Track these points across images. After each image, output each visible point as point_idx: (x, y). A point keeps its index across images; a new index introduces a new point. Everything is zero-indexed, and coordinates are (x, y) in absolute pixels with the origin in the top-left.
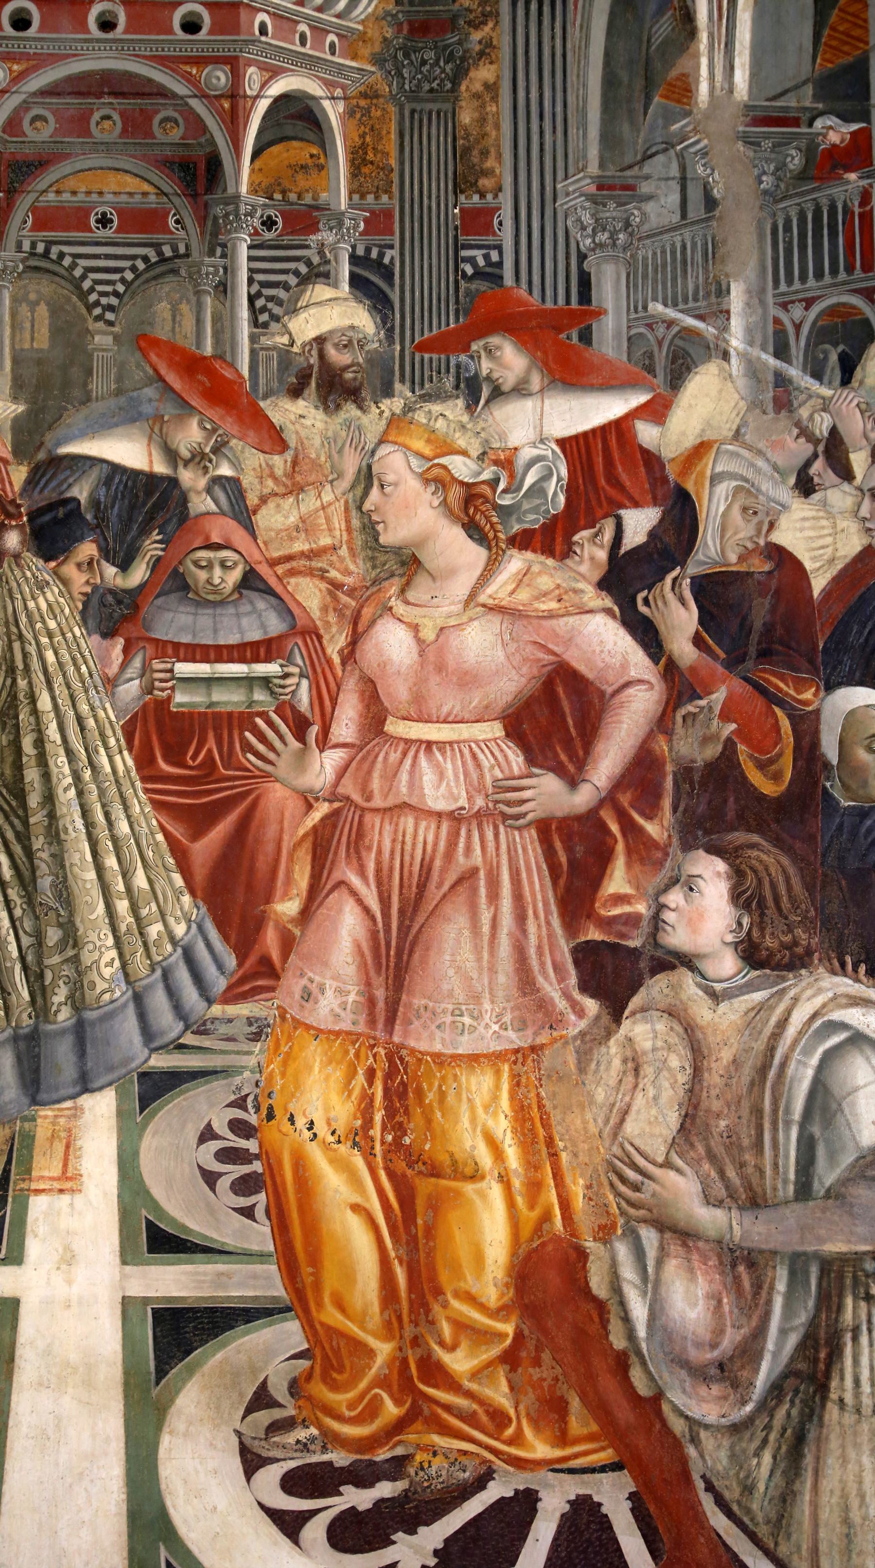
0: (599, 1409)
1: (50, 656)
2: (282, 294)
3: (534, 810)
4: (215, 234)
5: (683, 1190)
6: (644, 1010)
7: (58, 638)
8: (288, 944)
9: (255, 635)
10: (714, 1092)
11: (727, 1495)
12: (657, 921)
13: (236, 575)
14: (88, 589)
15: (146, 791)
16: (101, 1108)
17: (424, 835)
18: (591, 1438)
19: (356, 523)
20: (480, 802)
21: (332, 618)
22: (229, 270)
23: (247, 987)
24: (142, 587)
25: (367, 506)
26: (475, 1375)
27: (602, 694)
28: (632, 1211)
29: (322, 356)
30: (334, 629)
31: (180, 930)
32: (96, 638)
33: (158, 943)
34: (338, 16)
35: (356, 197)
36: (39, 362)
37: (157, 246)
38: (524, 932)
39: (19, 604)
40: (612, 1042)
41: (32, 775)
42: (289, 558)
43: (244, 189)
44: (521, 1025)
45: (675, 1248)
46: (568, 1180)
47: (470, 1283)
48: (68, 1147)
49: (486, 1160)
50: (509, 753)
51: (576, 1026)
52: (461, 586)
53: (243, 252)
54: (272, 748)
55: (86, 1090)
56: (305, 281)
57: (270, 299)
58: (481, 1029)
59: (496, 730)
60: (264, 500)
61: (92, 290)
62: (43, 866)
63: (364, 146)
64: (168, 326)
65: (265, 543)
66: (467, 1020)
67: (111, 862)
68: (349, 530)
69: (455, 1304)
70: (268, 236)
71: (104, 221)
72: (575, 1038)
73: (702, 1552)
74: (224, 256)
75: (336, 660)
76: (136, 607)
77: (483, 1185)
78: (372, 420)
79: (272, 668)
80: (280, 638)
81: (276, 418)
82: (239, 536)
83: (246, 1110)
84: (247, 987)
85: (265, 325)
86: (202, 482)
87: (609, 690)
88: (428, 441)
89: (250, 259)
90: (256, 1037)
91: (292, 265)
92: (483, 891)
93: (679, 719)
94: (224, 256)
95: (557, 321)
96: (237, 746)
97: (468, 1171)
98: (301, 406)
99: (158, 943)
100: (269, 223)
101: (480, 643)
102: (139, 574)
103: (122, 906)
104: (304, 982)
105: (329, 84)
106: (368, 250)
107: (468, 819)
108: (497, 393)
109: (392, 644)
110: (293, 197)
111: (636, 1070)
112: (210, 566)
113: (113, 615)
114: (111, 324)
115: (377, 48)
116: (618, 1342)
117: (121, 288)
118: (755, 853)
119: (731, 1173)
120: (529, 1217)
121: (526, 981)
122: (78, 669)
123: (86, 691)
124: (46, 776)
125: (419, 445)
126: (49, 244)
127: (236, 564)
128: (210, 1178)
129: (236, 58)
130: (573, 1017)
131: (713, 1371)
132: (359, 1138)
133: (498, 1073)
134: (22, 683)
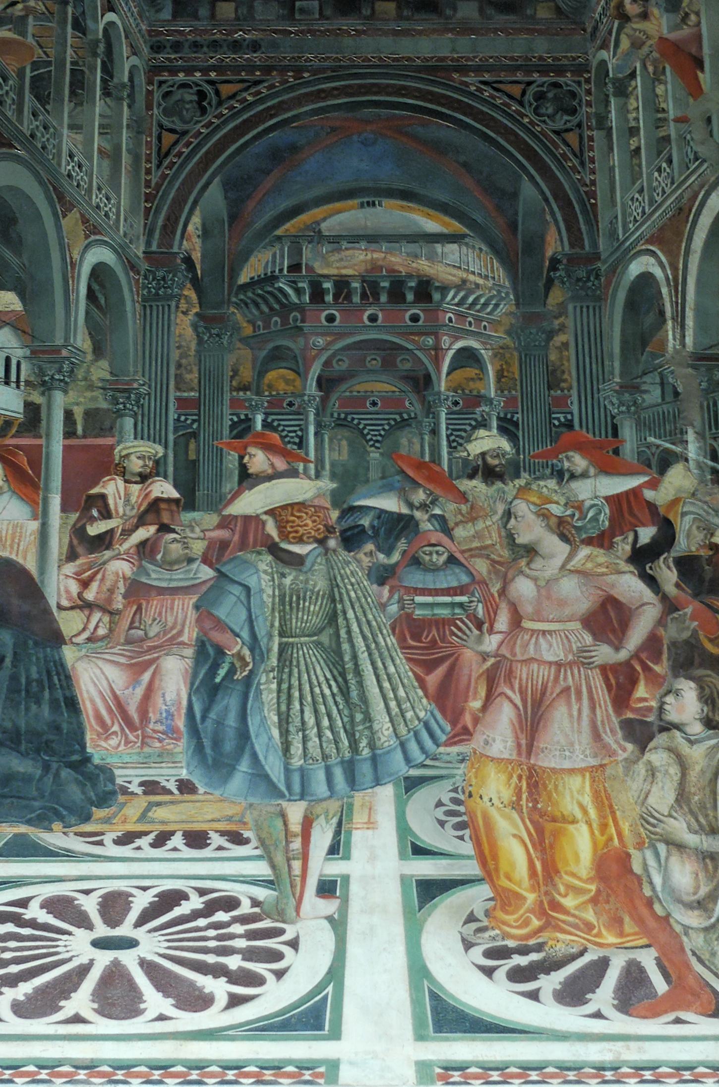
0: (639, 921)
1: (353, 594)
2: (463, 434)
3: (598, 661)
4: (430, 407)
5: (679, 827)
6: (655, 748)
7: (356, 586)
8: (476, 721)
9: (455, 584)
10: (692, 784)
11: (703, 957)
12: (661, 710)
13: (444, 557)
14: (370, 564)
15: (403, 653)
16: (386, 794)
17: (542, 674)
18: (635, 934)
19: (503, 534)
20: (570, 657)
21: (493, 576)
22: (437, 424)
23: (456, 739)
24: (397, 564)
25: (509, 526)
26: (577, 908)
27: (630, 609)
28: (652, 836)
29: (484, 460)
30: (494, 581)
31: (422, 714)
32: (375, 586)
33: (411, 721)
34: (487, 314)
35: (499, 392)
36: (343, 465)
37: (400, 414)
38: (595, 715)
39: (336, 572)
40: (640, 763)
41: (346, 646)
42: (470, 550)
43: (443, 389)
44: (595, 756)
45: (674, 851)
46: (621, 823)
47: (573, 868)
48: (370, 809)
49: (579, 814)
50: (585, 636)
51: (622, 756)
52: (558, 562)
53: (443, 416)
54: (465, 634)
55: (378, 784)
56: (474, 428)
57: (457, 436)
58: (574, 757)
59: (577, 625)
60: (457, 524)
61: (368, 434)
62: (353, 687)
63: (502, 370)
64: (407, 449)
65: (458, 543)
66: (567, 753)
67: (386, 685)
68: (500, 537)
69: (566, 877)
70: (455, 409)
71: (374, 404)
72: (621, 761)
73: (691, 981)
74: (433, 418)
75: (496, 595)
76: (395, 573)
77: (578, 825)
78: (510, 488)
79: (464, 599)
80: (467, 585)
81: (462, 488)
82: (445, 540)
83: (458, 793)
84: (456, 739)
85: (455, 448)
86: (426, 517)
87: (634, 607)
88: (539, 498)
89: (447, 419)
90: (462, 761)
91: (467, 422)
92: (573, 697)
93: (669, 621)
94: (433, 418)
95: (600, 446)
96: (448, 633)
97: (570, 819)
98: (474, 482)
99: (411, 721)
100: (456, 403)
101: (569, 586)
102: (396, 557)
103: (393, 704)
104: (485, 737)
105: (483, 343)
106: (506, 415)
107: (564, 665)
108: (573, 476)
109: (524, 588)
110: (467, 392)
111: (653, 775)
112: (431, 554)
113: (383, 576)
114: (379, 448)
115: (507, 328)
116: (647, 892)
117: (383, 433)
118: (709, 679)
119: (702, 820)
120: (602, 839)
121: (597, 736)
122: (366, 600)
123: (371, 609)
124: (353, 646)
125: (534, 499)
126: (347, 414)
127: (444, 553)
128: (442, 824)
129: (437, 333)
130: (620, 752)
131: (695, 904)
132: (516, 806)
133: (584, 776)
134: (339, 606)
